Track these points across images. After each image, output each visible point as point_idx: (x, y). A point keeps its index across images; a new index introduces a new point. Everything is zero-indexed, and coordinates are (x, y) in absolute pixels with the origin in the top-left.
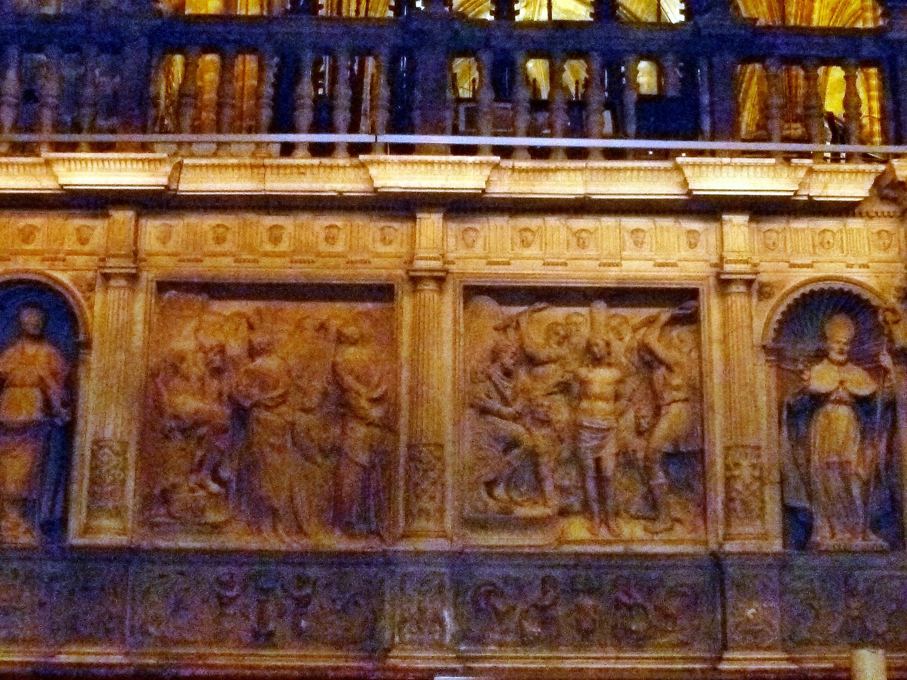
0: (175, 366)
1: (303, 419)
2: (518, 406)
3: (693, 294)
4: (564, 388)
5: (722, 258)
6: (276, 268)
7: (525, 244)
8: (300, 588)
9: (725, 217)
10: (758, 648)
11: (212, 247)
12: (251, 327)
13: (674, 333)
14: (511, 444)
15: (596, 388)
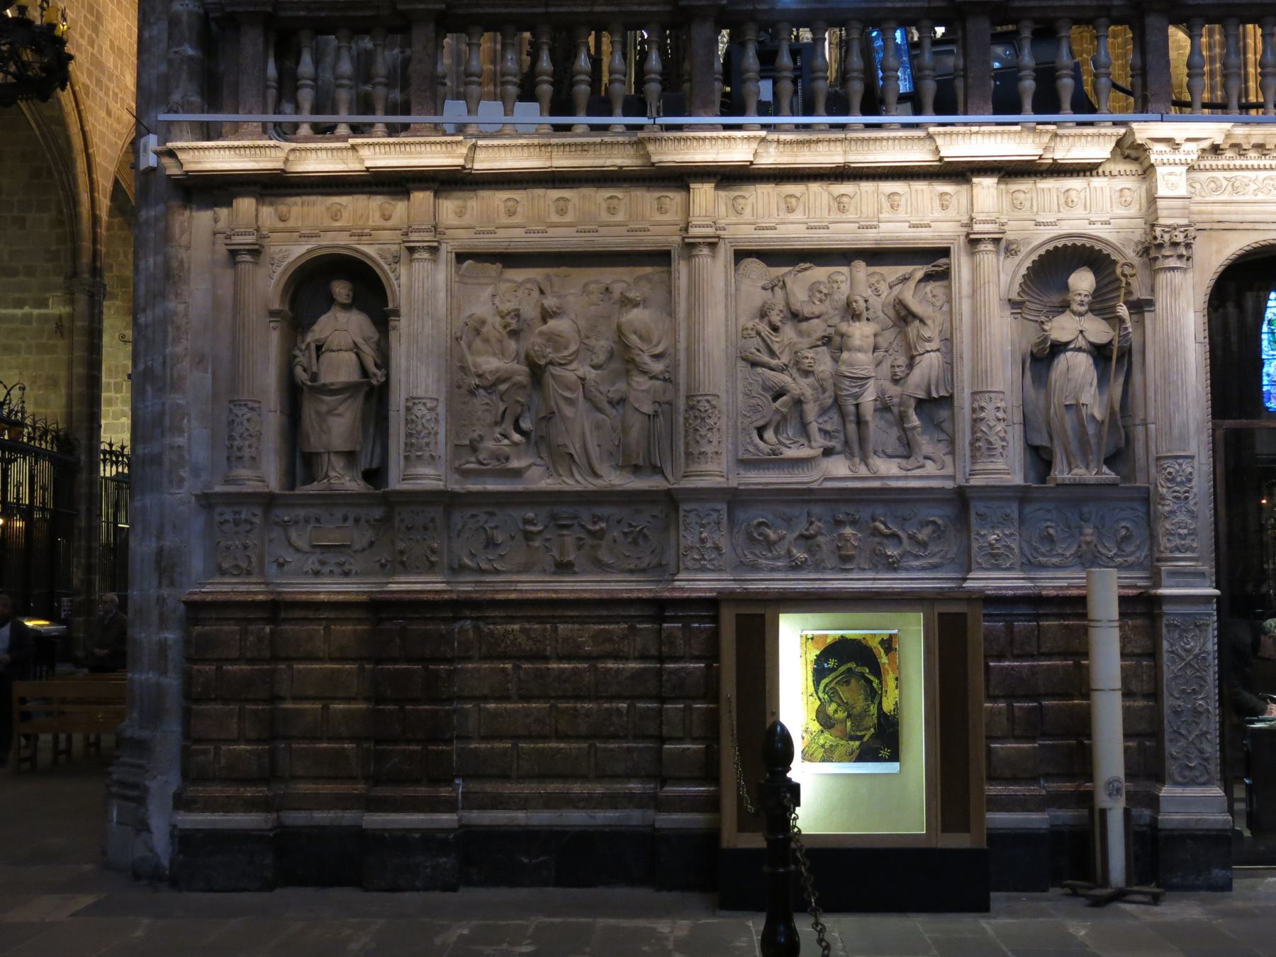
0: (477, 328)
1: (592, 374)
2: (785, 359)
3: (945, 252)
4: (827, 341)
5: (972, 219)
6: (564, 238)
7: (790, 210)
8: (595, 523)
9: (975, 180)
10: (998, 568)
11: (505, 220)
12: (542, 292)
13: (928, 289)
14: (779, 394)
15: (857, 342)
